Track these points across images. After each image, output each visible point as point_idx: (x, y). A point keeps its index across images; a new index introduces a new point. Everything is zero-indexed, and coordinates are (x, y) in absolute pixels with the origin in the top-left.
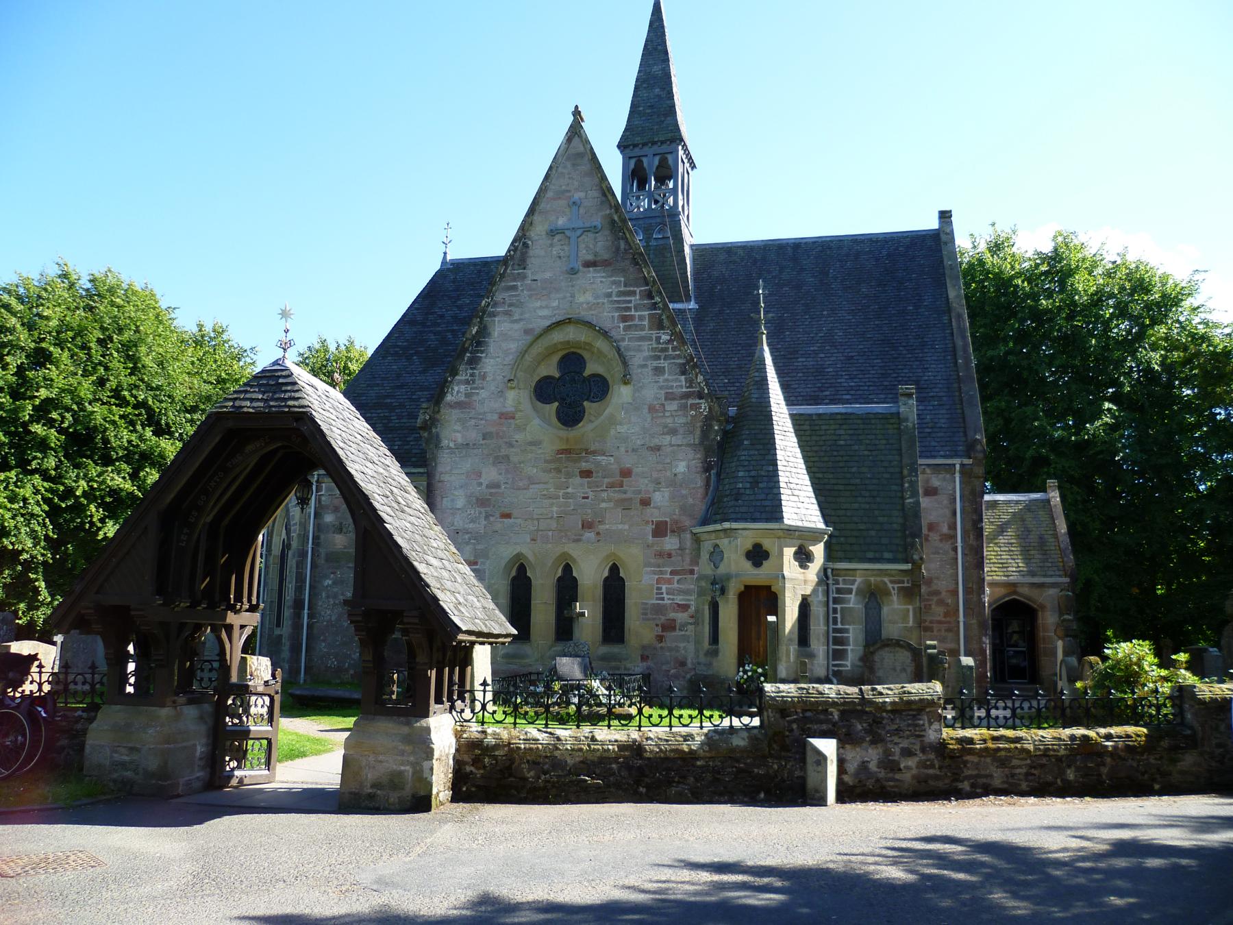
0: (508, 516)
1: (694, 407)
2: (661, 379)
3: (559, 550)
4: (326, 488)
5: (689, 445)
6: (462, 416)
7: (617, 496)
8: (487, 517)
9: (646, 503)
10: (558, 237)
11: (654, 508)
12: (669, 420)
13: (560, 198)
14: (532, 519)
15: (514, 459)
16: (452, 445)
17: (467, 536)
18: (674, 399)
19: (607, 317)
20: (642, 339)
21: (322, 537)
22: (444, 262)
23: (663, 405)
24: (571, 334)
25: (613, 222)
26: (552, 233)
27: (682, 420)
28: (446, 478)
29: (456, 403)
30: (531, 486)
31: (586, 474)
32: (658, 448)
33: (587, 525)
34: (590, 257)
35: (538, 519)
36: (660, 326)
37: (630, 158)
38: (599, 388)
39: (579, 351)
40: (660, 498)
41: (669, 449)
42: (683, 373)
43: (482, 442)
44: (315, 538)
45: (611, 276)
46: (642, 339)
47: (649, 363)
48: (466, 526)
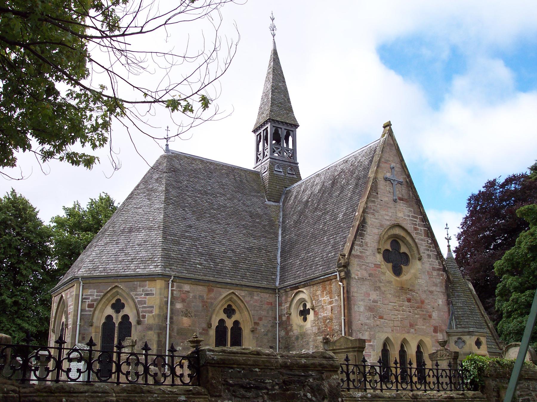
0: (381, 318)
1: (442, 275)
2: (430, 260)
3: (403, 337)
4: (176, 286)
5: (442, 292)
6: (359, 263)
7: (421, 313)
8: (374, 318)
9: (430, 316)
10: (388, 182)
11: (433, 319)
12: (434, 280)
13: (386, 163)
14: (391, 320)
15: (383, 289)
16: (356, 277)
17: (366, 327)
18: (435, 270)
19: (409, 227)
20: (422, 240)
21: (175, 318)
22: (167, 150)
23: (432, 272)
24: (397, 231)
25: (407, 182)
26: (386, 179)
27: (439, 281)
28: (355, 294)
29: (356, 255)
30: (390, 304)
31: (409, 300)
32: (431, 292)
33: (411, 326)
34: (400, 196)
35: (393, 321)
36: (428, 237)
37: (273, 126)
38: (405, 259)
39: (398, 240)
40: (435, 315)
41: (436, 293)
42: (437, 259)
43: (369, 278)
44: (171, 318)
45: (409, 207)
46: (422, 240)
47: (426, 252)
48: (365, 321)
